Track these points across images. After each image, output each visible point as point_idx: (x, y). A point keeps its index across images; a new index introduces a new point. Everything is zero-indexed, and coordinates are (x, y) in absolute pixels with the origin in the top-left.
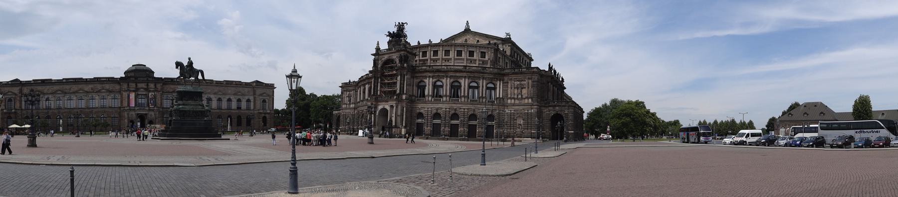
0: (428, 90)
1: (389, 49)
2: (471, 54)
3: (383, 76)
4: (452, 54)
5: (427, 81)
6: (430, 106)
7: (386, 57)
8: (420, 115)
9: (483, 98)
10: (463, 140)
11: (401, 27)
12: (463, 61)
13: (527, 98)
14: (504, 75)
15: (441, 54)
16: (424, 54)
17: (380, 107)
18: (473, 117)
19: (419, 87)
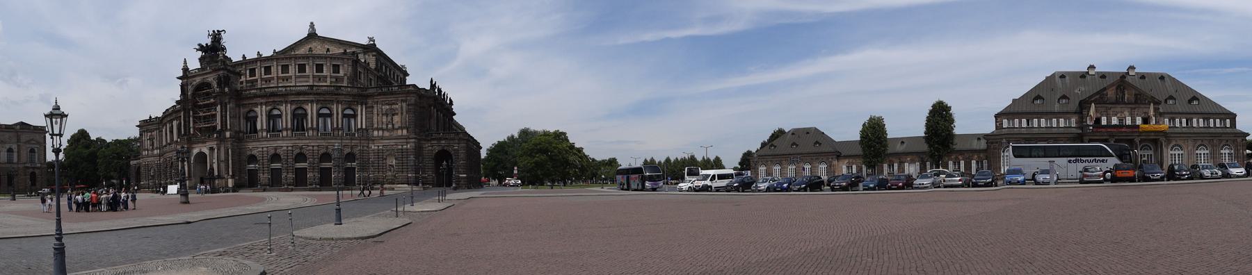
0: (261, 123)
1: (202, 69)
2: (320, 68)
3: (196, 106)
4: (292, 71)
5: (258, 110)
6: (265, 144)
8: (253, 159)
9: (338, 129)
10: (313, 190)
13: (401, 128)
15: (276, 71)
16: (253, 72)
17: (195, 151)
18: (326, 157)
19: (247, 119)
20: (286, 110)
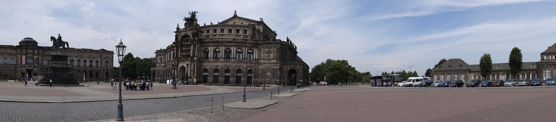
0: (211, 54)
1: (185, 28)
2: (238, 31)
3: (182, 45)
4: (226, 32)
5: (209, 48)
7: (184, 33)
8: (206, 70)
10: (233, 86)
11: (193, 15)
12: (233, 36)
13: (273, 59)
14: (259, 44)
15: (219, 31)
16: (208, 31)
17: (180, 65)
18: (239, 71)
19: (205, 52)
20: (222, 49)
